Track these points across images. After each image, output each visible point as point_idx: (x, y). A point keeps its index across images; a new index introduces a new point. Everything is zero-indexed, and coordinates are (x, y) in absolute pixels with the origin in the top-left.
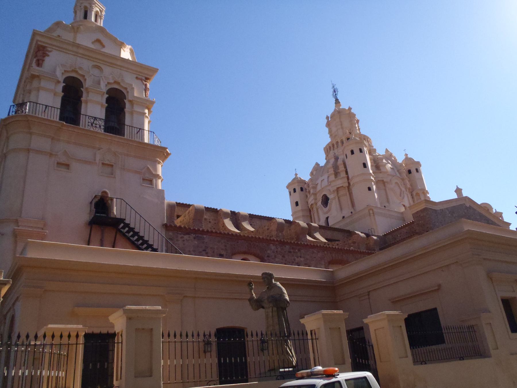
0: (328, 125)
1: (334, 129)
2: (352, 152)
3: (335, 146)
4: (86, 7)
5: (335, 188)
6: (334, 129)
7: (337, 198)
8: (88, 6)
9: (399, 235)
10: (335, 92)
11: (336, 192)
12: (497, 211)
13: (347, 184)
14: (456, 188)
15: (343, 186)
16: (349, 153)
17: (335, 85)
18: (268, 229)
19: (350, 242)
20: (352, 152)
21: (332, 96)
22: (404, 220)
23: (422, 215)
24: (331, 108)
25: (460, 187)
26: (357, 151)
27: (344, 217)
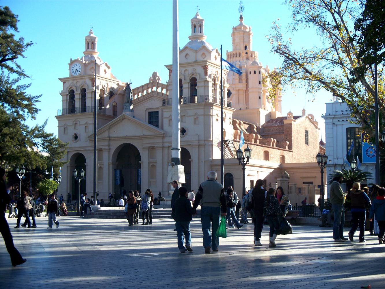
0: (233, 35)
1: (237, 40)
2: (255, 72)
3: (238, 55)
4: (200, 24)
5: (237, 89)
6: (237, 40)
7: (237, 95)
8: (201, 23)
9: (272, 130)
10: (241, 8)
11: (237, 91)
12: (316, 121)
13: (245, 89)
14: (321, 140)
15: (242, 89)
16: (252, 72)
17: (243, 3)
18: (248, 136)
19: (266, 140)
20: (255, 72)
21: (238, 10)
22: (270, 117)
23: (289, 126)
24: (237, 23)
25: (305, 109)
26: (257, 72)
27: (240, 109)
